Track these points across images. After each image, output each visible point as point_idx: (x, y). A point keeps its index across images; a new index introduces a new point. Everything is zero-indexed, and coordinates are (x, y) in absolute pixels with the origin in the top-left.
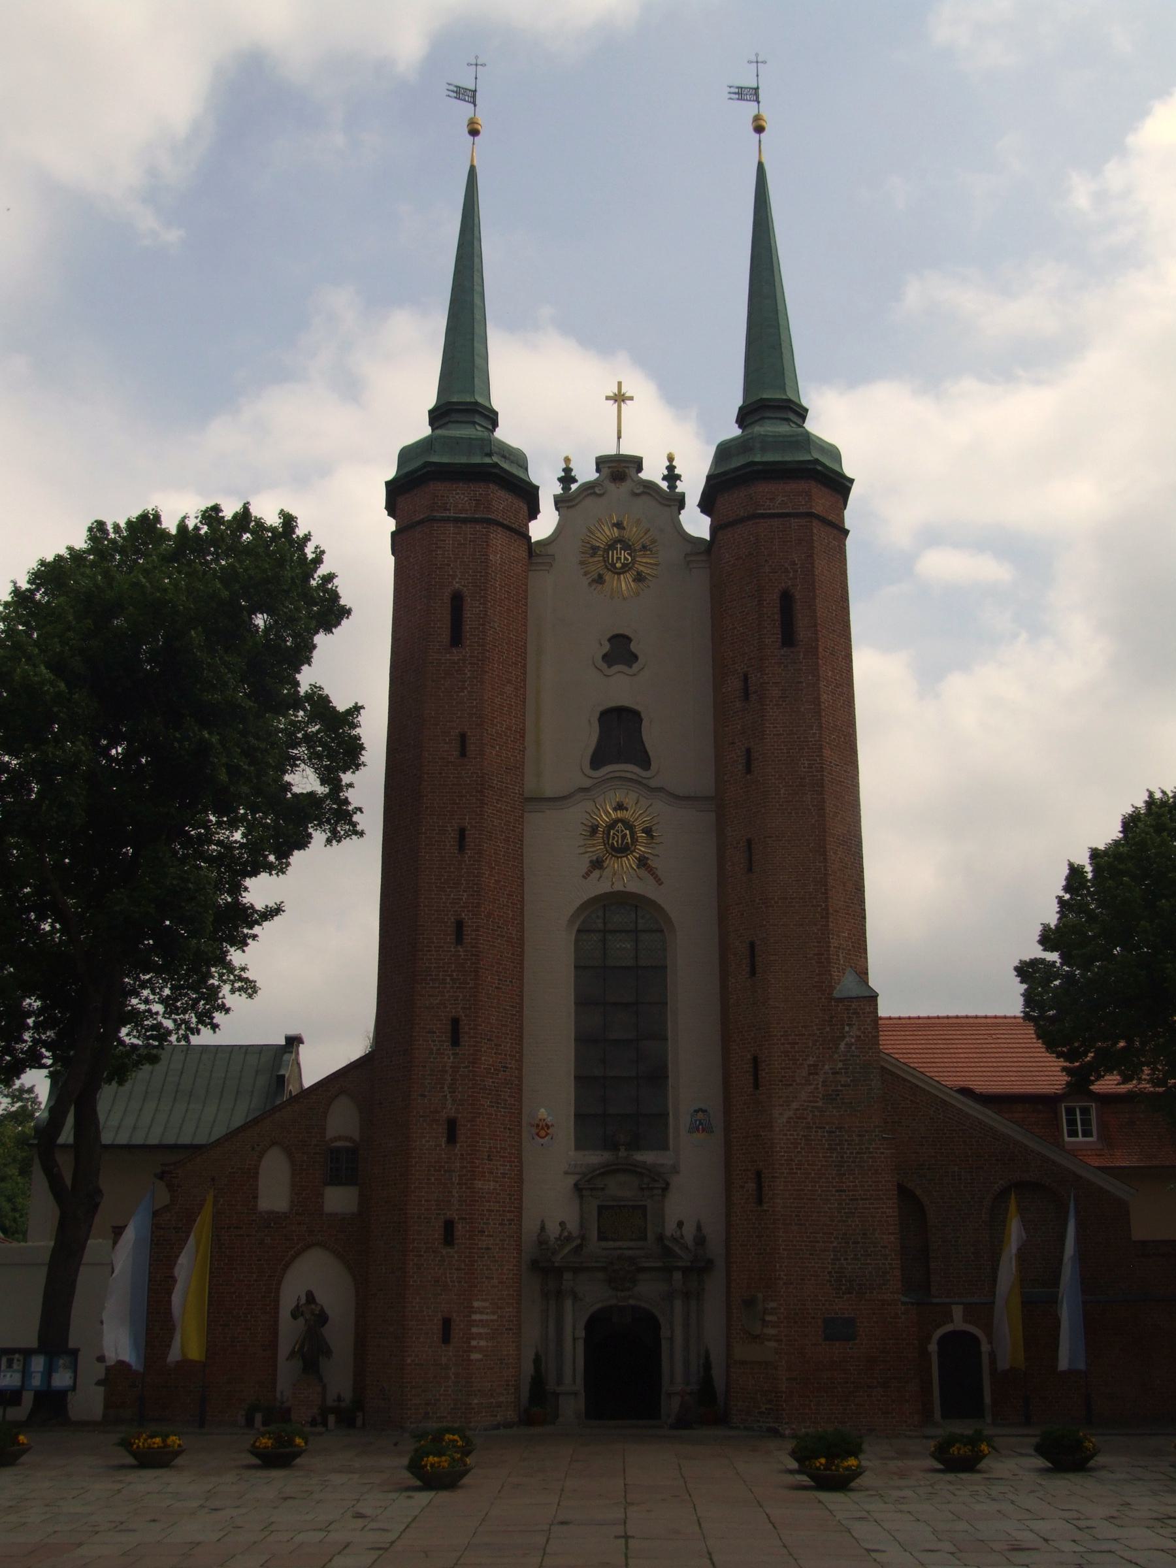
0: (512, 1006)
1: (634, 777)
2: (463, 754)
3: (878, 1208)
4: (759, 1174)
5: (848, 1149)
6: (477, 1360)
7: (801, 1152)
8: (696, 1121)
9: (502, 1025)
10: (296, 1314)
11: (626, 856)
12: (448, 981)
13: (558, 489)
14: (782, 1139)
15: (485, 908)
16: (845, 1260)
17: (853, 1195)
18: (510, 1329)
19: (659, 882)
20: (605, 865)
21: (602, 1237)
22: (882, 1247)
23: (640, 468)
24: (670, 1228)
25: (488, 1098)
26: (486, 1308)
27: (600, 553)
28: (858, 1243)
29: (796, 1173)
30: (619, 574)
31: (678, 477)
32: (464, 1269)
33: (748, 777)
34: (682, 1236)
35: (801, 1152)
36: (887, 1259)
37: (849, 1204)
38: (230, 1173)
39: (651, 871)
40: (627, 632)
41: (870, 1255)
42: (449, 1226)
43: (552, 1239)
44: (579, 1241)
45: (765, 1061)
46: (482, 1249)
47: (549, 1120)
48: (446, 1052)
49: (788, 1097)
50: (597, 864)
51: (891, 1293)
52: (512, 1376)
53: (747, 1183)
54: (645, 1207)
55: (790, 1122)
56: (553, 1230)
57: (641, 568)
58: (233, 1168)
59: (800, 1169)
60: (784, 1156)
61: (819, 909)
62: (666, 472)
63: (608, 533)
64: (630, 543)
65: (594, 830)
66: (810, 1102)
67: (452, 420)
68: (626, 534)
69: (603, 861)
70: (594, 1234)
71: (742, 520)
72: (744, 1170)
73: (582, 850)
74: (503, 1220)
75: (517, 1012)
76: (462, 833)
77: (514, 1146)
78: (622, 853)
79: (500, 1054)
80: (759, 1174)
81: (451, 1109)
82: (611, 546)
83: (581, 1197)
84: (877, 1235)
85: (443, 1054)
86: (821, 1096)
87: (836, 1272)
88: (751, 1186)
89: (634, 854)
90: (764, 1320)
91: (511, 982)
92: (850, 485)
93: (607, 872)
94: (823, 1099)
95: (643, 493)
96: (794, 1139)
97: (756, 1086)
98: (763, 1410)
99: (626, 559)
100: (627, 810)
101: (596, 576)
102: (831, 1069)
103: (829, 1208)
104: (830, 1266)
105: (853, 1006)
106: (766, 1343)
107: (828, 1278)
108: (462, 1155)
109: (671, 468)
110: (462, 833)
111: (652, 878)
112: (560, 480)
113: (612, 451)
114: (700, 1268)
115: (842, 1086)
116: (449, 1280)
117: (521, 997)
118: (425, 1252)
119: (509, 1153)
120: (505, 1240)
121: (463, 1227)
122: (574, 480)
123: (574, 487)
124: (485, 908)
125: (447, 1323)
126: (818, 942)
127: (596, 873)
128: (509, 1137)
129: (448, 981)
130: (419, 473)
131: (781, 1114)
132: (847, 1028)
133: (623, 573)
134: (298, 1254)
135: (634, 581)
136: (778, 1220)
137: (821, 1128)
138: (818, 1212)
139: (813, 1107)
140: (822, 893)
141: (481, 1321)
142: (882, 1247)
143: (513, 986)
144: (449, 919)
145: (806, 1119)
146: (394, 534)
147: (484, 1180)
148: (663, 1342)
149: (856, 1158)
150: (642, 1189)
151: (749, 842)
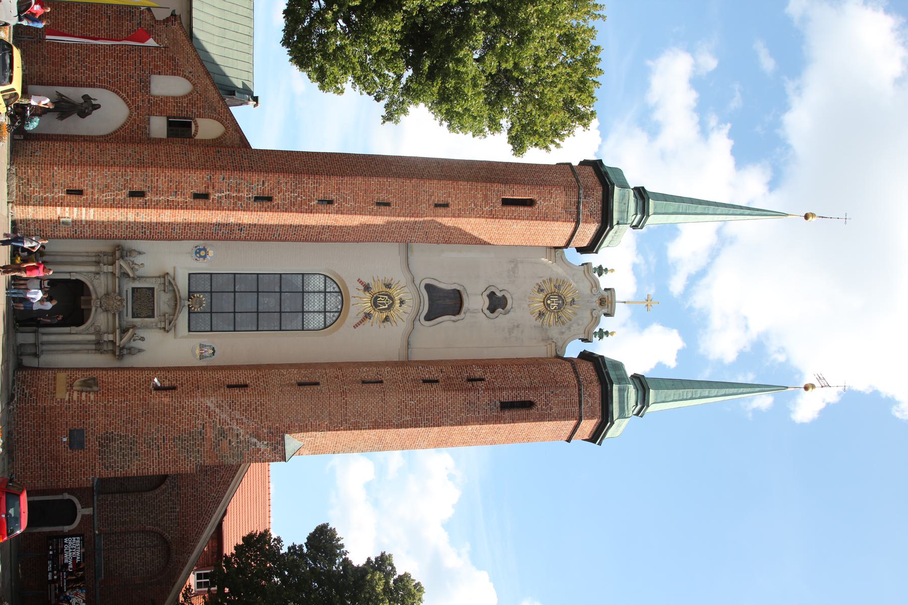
1: (420, 311)
2: (437, 206)
4: (174, 388)
5: (190, 444)
6: (56, 211)
7: (188, 414)
9: (267, 230)
10: (86, 98)
11: (372, 306)
12: (295, 195)
13: (595, 265)
15: (341, 218)
16: (121, 442)
17: (161, 447)
18: (76, 233)
21: (133, 289)
22: (129, 466)
23: (606, 315)
24: (141, 333)
28: (131, 450)
29: (175, 412)
31: (601, 338)
32: (114, 203)
33: (421, 381)
34: (134, 340)
35: (188, 414)
37: (155, 444)
38: (175, 58)
40: (509, 307)
41: (123, 458)
42: (141, 194)
43: (132, 259)
44: (131, 275)
45: (245, 392)
46: (127, 215)
47: (208, 257)
49: (223, 406)
50: (367, 288)
51: (100, 471)
52: (46, 234)
53: (169, 380)
54: (153, 316)
56: (139, 260)
57: (547, 316)
58: (178, 59)
59: (178, 414)
60: (186, 404)
62: (604, 331)
63: (568, 296)
64: (562, 309)
67: (639, 201)
68: (568, 306)
70: (137, 285)
72: (176, 379)
73: (376, 280)
75: (276, 238)
76: (388, 204)
77: (192, 235)
78: (374, 302)
80: (174, 388)
81: (215, 196)
83: (159, 277)
86: (224, 427)
87: (112, 437)
89: (373, 311)
90: (82, 392)
91: (295, 234)
93: (361, 293)
95: (593, 317)
97: (229, 386)
98: (25, 391)
99: (553, 307)
101: (543, 287)
102: (240, 433)
104: (116, 433)
106: (68, 393)
109: (607, 333)
111: (358, 321)
112: (600, 267)
113: (617, 299)
116: (107, 194)
117: (285, 240)
118: (125, 179)
119: (187, 232)
120: (132, 229)
121: (141, 202)
122: (600, 275)
123: (596, 275)
124: (341, 218)
125: (80, 192)
126: (319, 425)
127: (362, 288)
128: (198, 232)
129: (295, 195)
132: (266, 443)
133: (544, 304)
134: (124, 99)
135: (540, 311)
136: (146, 401)
137: (203, 427)
138: (150, 425)
140: (349, 427)
142: (129, 466)
143: (292, 235)
145: (209, 417)
146: (570, 164)
148: (69, 328)
149: (185, 449)
150: (165, 315)
151: (381, 382)
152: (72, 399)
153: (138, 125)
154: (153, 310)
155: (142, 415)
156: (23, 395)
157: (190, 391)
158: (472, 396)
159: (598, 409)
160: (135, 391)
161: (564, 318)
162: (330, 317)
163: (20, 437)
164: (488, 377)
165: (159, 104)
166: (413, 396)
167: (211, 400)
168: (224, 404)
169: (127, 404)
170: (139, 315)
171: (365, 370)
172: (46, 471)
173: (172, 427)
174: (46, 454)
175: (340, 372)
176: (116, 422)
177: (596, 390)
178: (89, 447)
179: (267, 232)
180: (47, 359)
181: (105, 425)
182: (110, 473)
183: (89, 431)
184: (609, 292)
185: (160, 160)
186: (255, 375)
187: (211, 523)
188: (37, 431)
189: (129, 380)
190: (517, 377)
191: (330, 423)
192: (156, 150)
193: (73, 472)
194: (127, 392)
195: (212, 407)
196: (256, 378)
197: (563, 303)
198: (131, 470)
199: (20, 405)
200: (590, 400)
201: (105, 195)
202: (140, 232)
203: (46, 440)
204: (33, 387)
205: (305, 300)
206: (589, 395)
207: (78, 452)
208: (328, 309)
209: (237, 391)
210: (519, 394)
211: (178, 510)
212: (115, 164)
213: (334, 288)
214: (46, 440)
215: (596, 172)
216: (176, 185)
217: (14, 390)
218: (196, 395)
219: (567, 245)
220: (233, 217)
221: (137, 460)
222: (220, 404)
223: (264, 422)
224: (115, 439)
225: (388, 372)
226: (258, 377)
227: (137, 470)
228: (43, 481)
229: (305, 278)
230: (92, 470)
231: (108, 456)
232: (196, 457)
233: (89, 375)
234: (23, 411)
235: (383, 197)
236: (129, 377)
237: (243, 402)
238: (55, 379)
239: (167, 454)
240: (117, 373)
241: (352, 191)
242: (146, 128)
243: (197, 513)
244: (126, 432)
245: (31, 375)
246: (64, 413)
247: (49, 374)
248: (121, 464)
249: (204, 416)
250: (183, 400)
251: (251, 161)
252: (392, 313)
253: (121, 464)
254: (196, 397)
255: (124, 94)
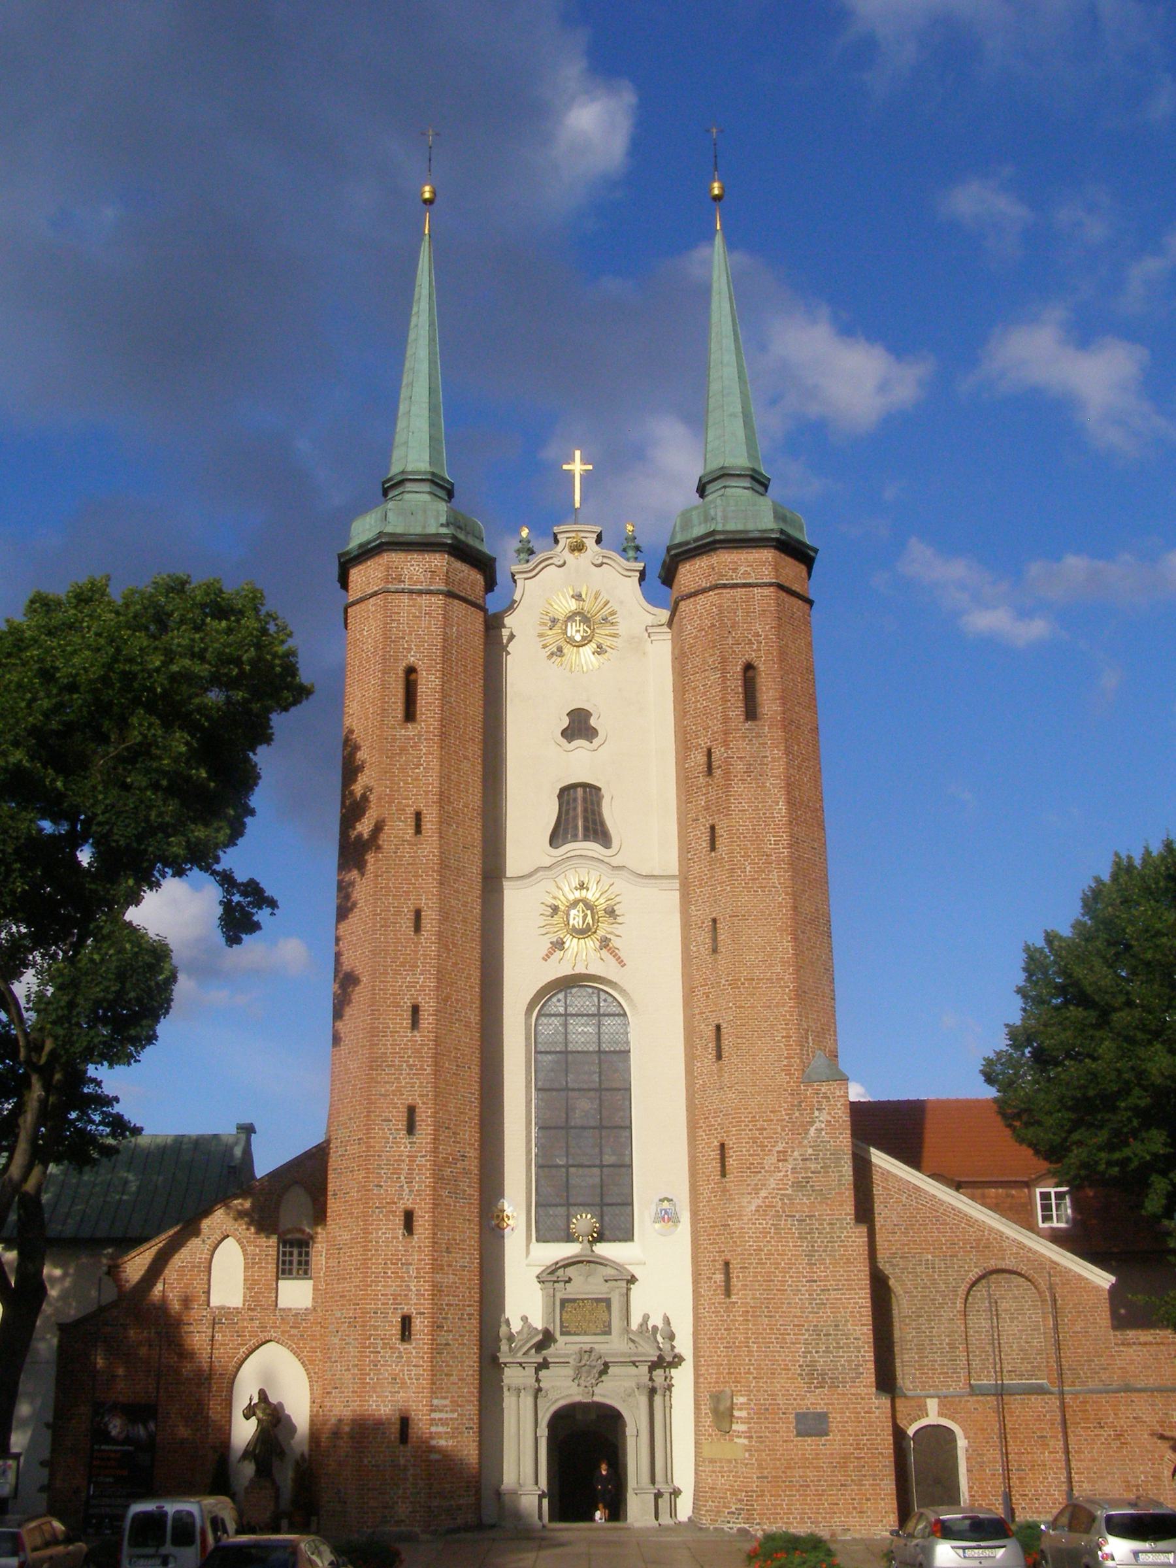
0: (471, 1093)
2: (418, 830)
3: (849, 1299)
4: (727, 1264)
8: (661, 1210)
9: (461, 1113)
10: (249, 1413)
12: (404, 1067)
14: (751, 1228)
16: (817, 1352)
17: (825, 1285)
18: (471, 1428)
19: (622, 963)
20: (566, 946)
22: (855, 1339)
25: (445, 1188)
26: (446, 1406)
27: (559, 625)
28: (830, 1335)
30: (578, 646)
33: (713, 854)
36: (859, 1352)
39: (613, 952)
41: (842, 1348)
42: (406, 1322)
48: (403, 1141)
49: (757, 1185)
53: (714, 1274)
54: (610, 1299)
55: (758, 1211)
59: (770, 1259)
61: (787, 990)
63: (566, 605)
64: (589, 616)
65: (555, 909)
66: (780, 1189)
69: (564, 943)
71: (704, 591)
72: (712, 1261)
73: (543, 931)
74: (462, 1314)
76: (418, 914)
79: (459, 1143)
80: (727, 1264)
81: (408, 1200)
82: (570, 618)
84: (850, 1327)
85: (400, 1142)
86: (790, 1183)
87: (807, 1366)
88: (719, 1277)
91: (469, 1068)
92: (812, 554)
94: (793, 1186)
96: (764, 1228)
97: (723, 1174)
98: (733, 1510)
99: (585, 631)
100: (588, 890)
102: (801, 1155)
103: (799, 1299)
104: (802, 1359)
105: (823, 1091)
106: (736, 1440)
107: (799, 1372)
108: (420, 1247)
110: (418, 914)
114: (665, 1362)
115: (812, 1172)
116: (406, 1377)
119: (469, 1245)
121: (420, 1322)
127: (559, 954)
129: (404, 1067)
130: (374, 544)
131: (749, 1202)
132: (817, 1113)
136: (748, 1312)
137: (791, 1216)
138: (788, 1303)
139: (782, 1195)
141: (440, 1419)
142: (855, 1339)
144: (406, 1003)
145: (775, 1207)
147: (443, 1274)
149: (827, 1246)
151: (714, 921)
152: (746, 1432)
153: (291, 1327)
154: (598, 1300)
155: (771, 1317)
156: (740, 1514)
157: (732, 1238)
158: (740, 766)
159: (757, 556)
160: (731, 1329)
161: (605, 612)
162: (608, 1006)
163: (809, 1518)
164: (704, 742)
165: (255, 1293)
166: (739, 868)
167: (745, 1204)
168: (753, 1183)
169: (753, 1342)
170: (607, 1324)
171: (695, 949)
172: (865, 1476)
173: (791, 1268)
174: (837, 1476)
175: (699, 991)
176: (782, 1361)
177: (723, 559)
178: (825, 1404)
179: (466, 1113)
180: (684, 1475)
181: (788, 1378)
182: (868, 1369)
183: (798, 1404)
184: (559, 536)
185: (350, 1291)
186: (704, 1131)
187: (952, 1203)
188: (798, 1491)
189: (714, 1338)
190: (705, 693)
191: (783, 1006)
192: (332, 1297)
193: (867, 1431)
194: (734, 1343)
195: (759, 1201)
196: (710, 1130)
197: (579, 613)
198: (862, 1334)
199: (755, 1519)
200: (742, 569)
201: (409, 1381)
202: (469, 1323)
203: (815, 1476)
204: (726, 1498)
205: (580, 1049)
206: (734, 570)
207: (832, 1422)
208: (593, 1010)
209: (731, 1162)
210: (732, 690)
211: (930, 1257)
212: (357, 1365)
213: (559, 1001)
214: (815, 1476)
215: (360, 563)
216: (392, 1264)
217: (730, 1528)
218: (738, 1229)
219: (482, 609)
220: (442, 1171)
221: (846, 1325)
222: (753, 1189)
223: (782, 1116)
224: (811, 1361)
225: (697, 911)
226: (707, 1126)
227: (862, 1325)
228: (882, 1480)
229: (543, 1050)
230: (862, 1399)
231: (840, 1374)
232: (841, 1228)
233: (705, 1404)
234: (765, 1514)
235: (407, 923)
236: (709, 1339)
237: (749, 1151)
238: (712, 1461)
239: (835, 1276)
240: (702, 1359)
241: (396, 972)
242: (297, 1315)
243: (936, 1224)
244: (800, 1343)
245: (707, 1501)
246: (768, 1446)
247: (705, 1471)
248: (852, 1352)
249: (773, 1216)
250: (746, 1250)
251: (349, 1141)
252: (602, 904)
253: (852, 1352)
254: (742, 1228)
255: (241, 1351)
